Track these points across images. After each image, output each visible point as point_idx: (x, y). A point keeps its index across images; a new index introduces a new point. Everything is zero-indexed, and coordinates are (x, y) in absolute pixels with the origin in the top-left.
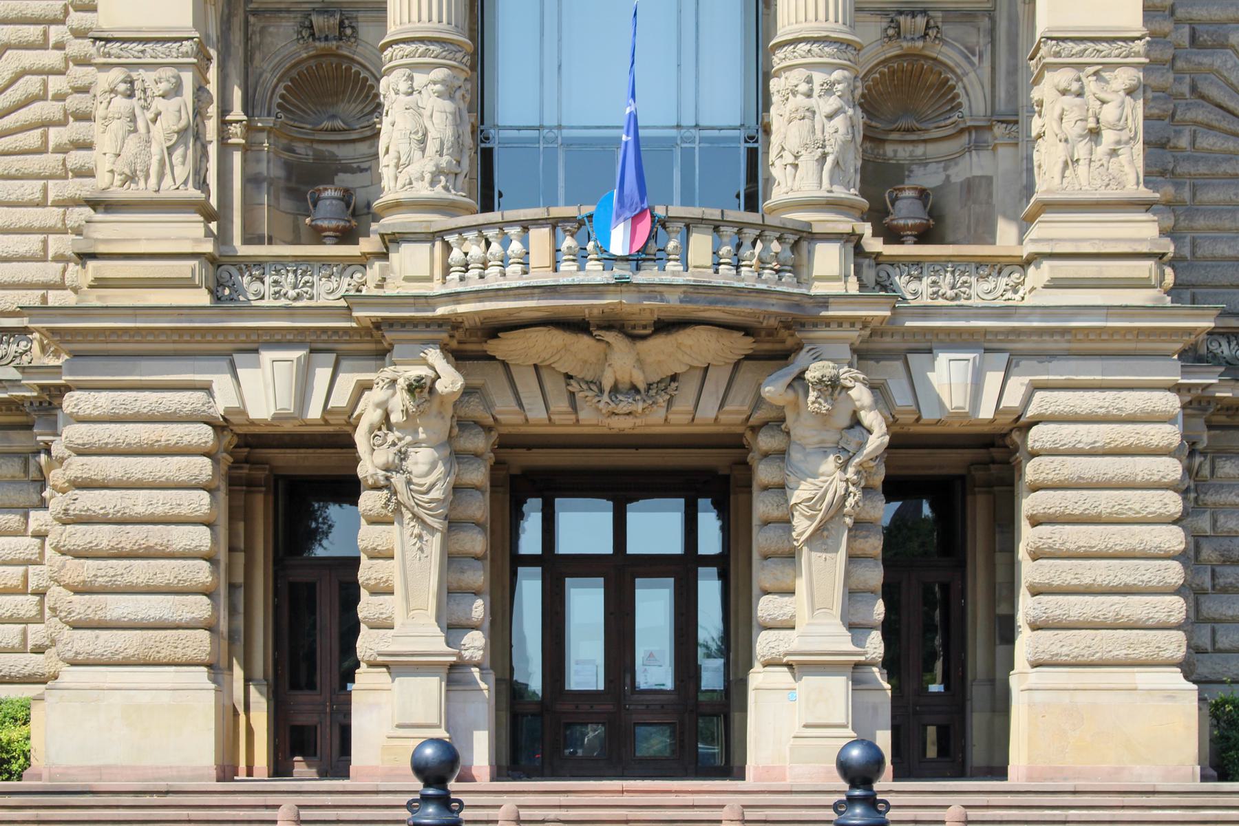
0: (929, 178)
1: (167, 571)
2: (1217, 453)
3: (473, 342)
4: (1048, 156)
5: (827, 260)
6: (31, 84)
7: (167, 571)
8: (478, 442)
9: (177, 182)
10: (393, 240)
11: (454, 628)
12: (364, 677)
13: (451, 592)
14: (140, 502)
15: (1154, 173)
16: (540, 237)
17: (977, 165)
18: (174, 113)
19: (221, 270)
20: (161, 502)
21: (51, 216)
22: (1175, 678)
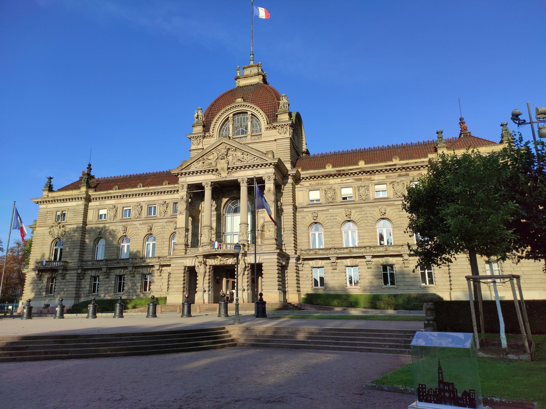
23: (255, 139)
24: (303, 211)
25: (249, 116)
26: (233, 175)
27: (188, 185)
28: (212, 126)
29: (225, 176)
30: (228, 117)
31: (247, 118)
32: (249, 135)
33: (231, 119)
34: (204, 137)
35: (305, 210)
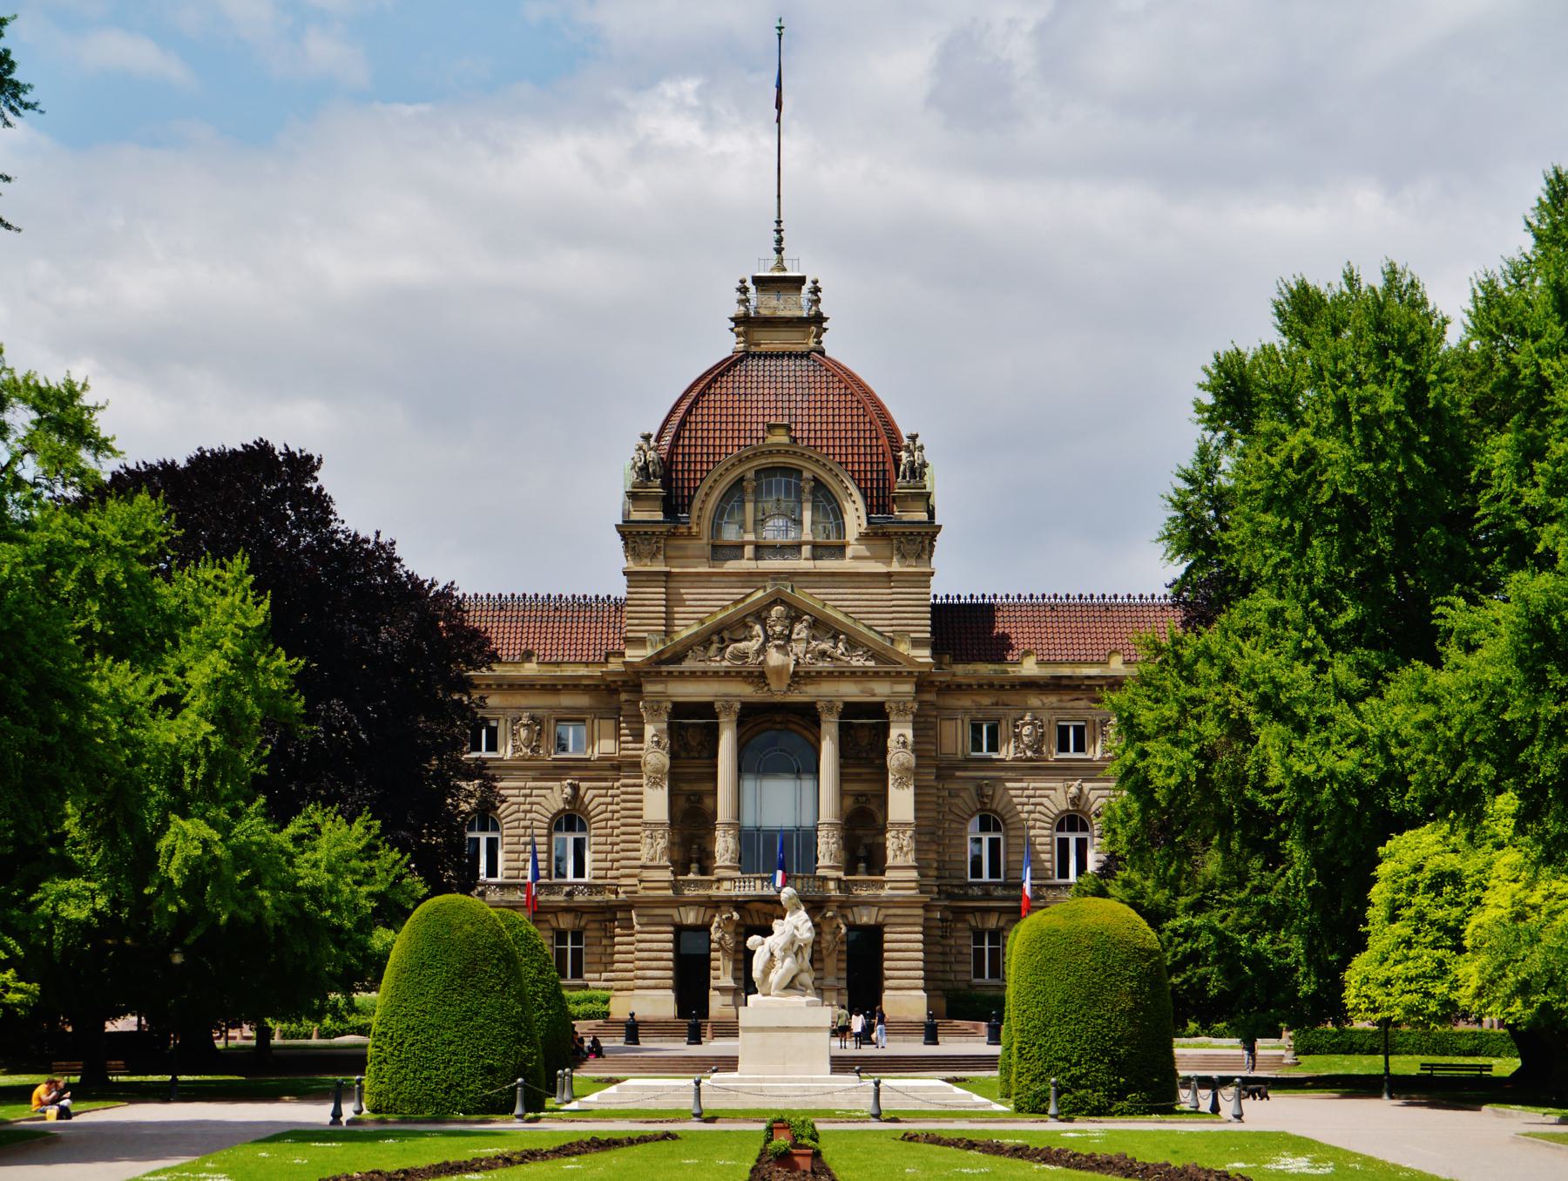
0: (867, 841)
1: (662, 964)
2: (956, 920)
3: (739, 905)
4: (890, 853)
5: (832, 885)
6: (602, 807)
7: (662, 964)
8: (742, 930)
9: (665, 862)
10: (719, 880)
11: (735, 979)
12: (712, 993)
13: (735, 969)
14: (655, 946)
15: (917, 860)
16: (759, 883)
17: (880, 840)
18: (662, 843)
19: (675, 886)
20: (661, 945)
21: (609, 848)
22: (922, 993)
23: (820, 558)
24: (952, 777)
25: (807, 487)
26: (804, 688)
27: (675, 704)
28: (696, 504)
29: (778, 692)
30: (742, 479)
31: (800, 491)
32: (806, 543)
33: (749, 486)
34: (673, 535)
35: (958, 774)
